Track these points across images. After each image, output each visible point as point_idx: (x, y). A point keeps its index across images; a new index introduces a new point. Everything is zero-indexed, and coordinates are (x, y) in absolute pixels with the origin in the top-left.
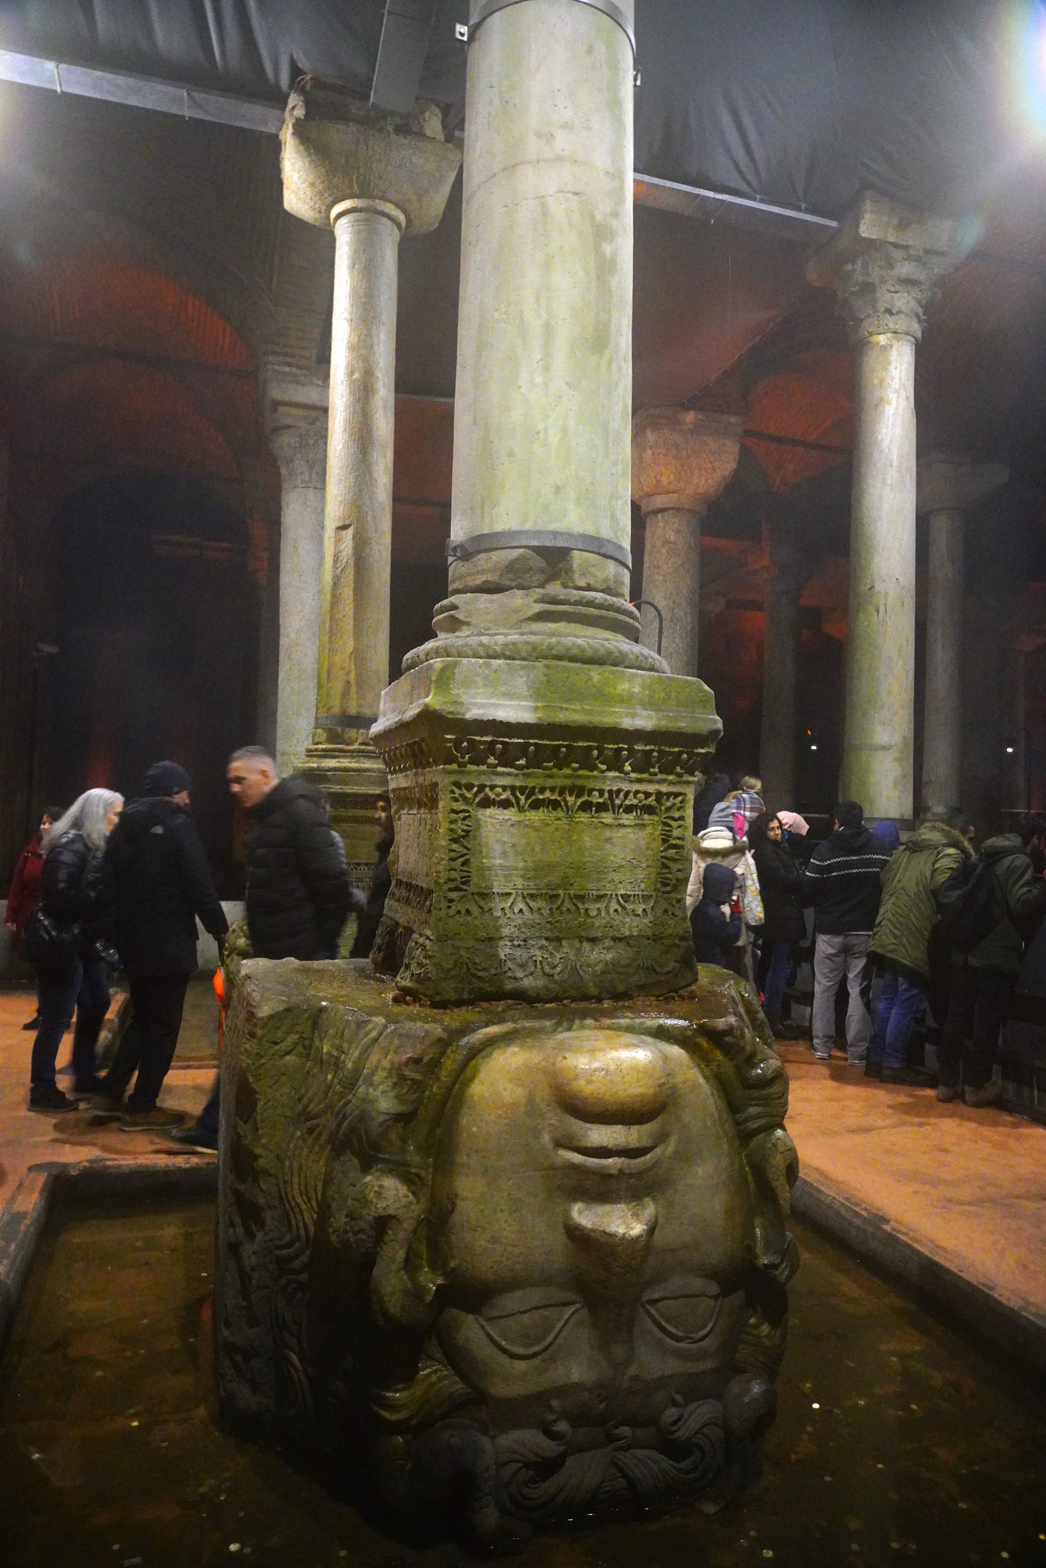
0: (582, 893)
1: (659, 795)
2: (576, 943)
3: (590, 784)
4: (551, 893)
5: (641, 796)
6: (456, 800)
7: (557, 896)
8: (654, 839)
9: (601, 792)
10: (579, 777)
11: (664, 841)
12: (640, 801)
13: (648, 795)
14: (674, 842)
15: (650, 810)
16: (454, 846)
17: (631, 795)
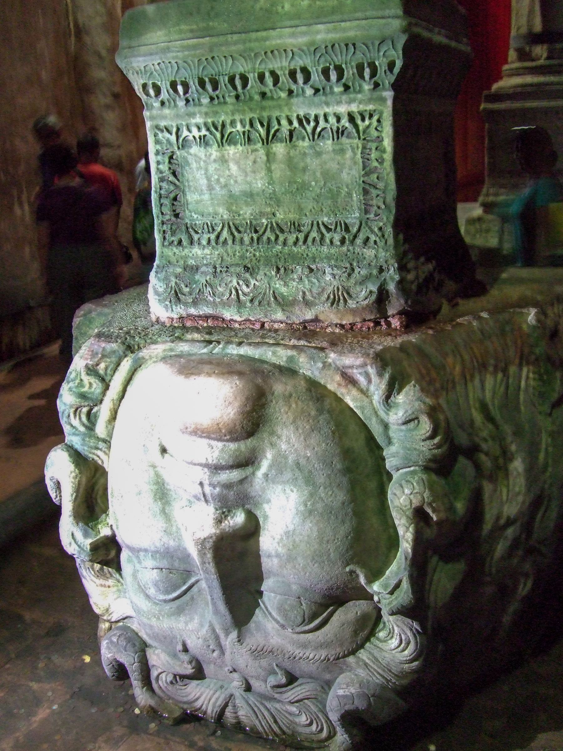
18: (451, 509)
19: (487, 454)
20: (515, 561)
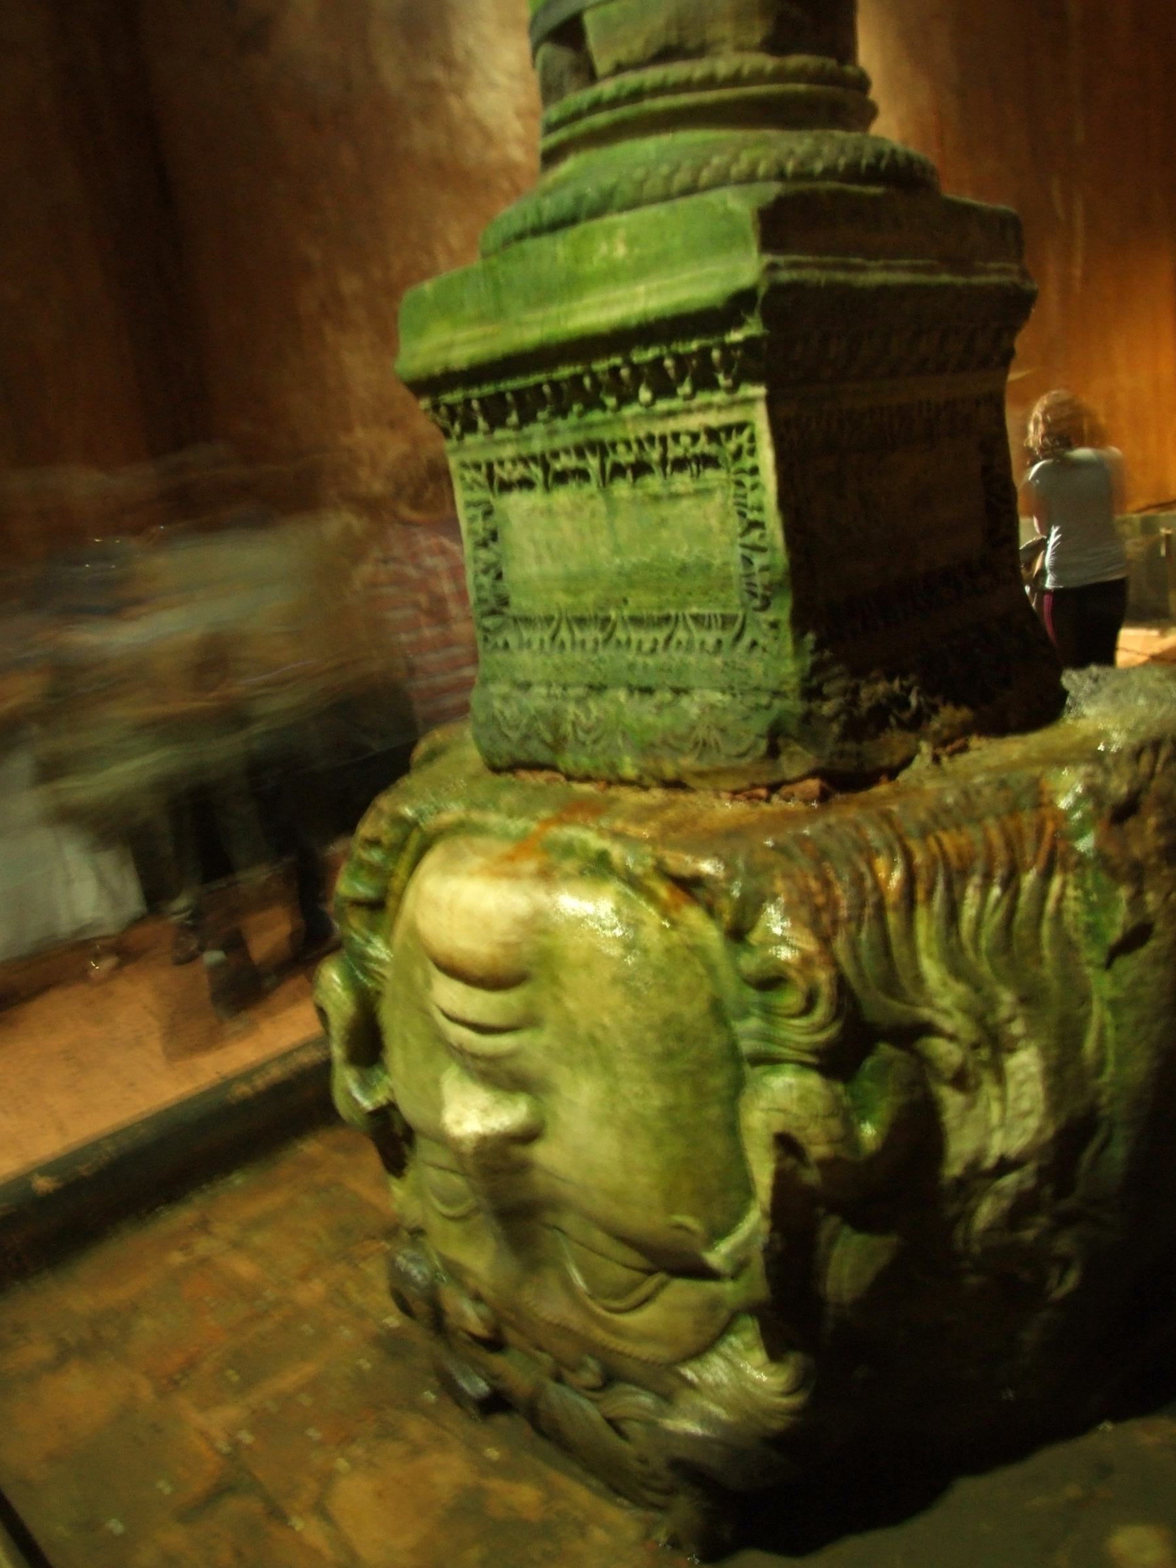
0: (637, 613)
1: (713, 434)
2: (622, 695)
3: (606, 435)
4: (601, 614)
5: (685, 440)
6: (471, 488)
7: (607, 620)
8: (728, 514)
9: (628, 444)
10: (590, 426)
11: (742, 515)
12: (686, 450)
13: (695, 437)
14: (752, 516)
15: (708, 461)
16: (483, 554)
17: (670, 442)
18: (849, 1137)
19: (952, 1038)
20: (1029, 1235)
